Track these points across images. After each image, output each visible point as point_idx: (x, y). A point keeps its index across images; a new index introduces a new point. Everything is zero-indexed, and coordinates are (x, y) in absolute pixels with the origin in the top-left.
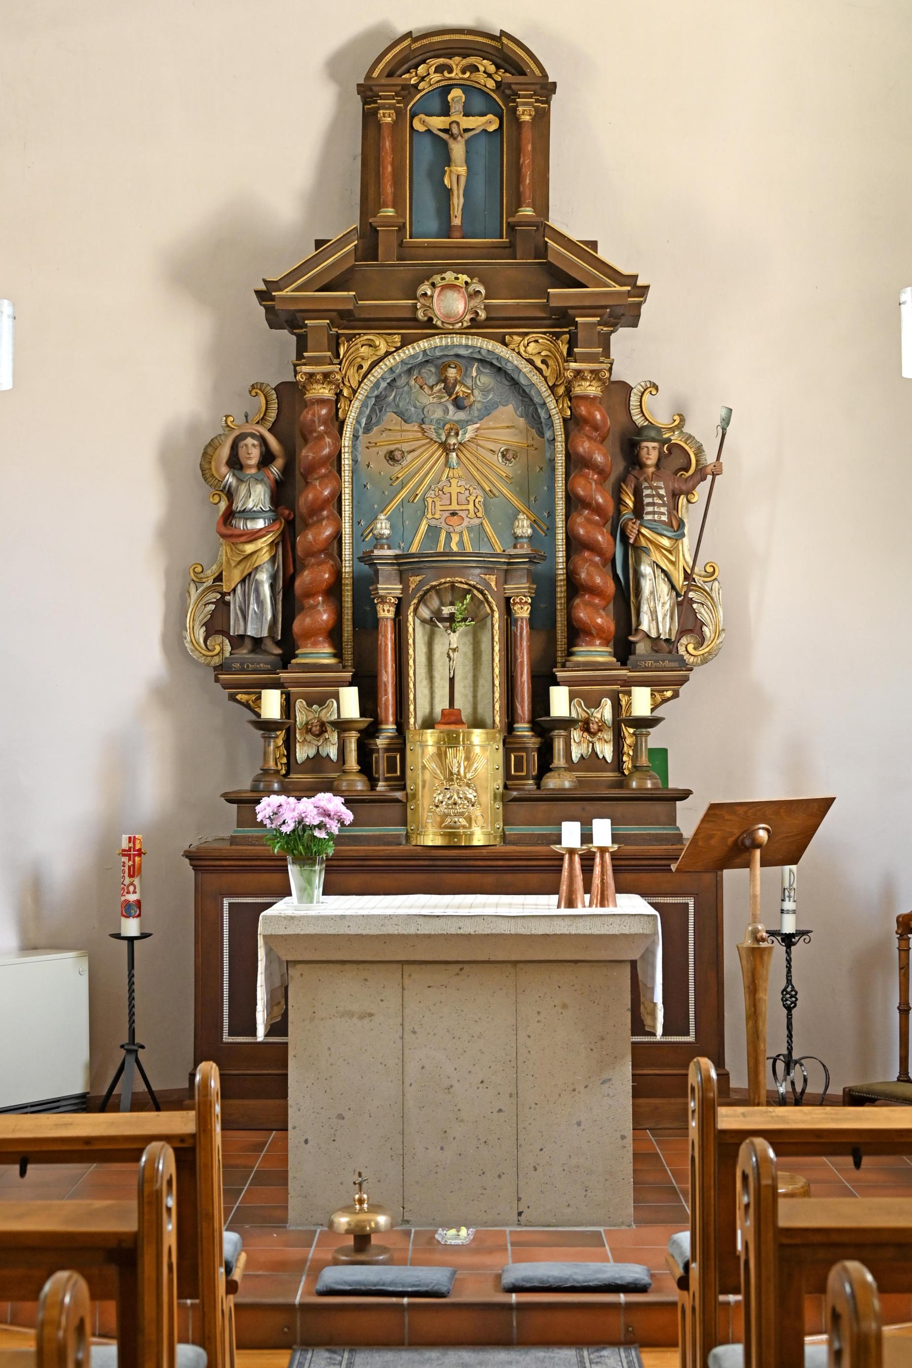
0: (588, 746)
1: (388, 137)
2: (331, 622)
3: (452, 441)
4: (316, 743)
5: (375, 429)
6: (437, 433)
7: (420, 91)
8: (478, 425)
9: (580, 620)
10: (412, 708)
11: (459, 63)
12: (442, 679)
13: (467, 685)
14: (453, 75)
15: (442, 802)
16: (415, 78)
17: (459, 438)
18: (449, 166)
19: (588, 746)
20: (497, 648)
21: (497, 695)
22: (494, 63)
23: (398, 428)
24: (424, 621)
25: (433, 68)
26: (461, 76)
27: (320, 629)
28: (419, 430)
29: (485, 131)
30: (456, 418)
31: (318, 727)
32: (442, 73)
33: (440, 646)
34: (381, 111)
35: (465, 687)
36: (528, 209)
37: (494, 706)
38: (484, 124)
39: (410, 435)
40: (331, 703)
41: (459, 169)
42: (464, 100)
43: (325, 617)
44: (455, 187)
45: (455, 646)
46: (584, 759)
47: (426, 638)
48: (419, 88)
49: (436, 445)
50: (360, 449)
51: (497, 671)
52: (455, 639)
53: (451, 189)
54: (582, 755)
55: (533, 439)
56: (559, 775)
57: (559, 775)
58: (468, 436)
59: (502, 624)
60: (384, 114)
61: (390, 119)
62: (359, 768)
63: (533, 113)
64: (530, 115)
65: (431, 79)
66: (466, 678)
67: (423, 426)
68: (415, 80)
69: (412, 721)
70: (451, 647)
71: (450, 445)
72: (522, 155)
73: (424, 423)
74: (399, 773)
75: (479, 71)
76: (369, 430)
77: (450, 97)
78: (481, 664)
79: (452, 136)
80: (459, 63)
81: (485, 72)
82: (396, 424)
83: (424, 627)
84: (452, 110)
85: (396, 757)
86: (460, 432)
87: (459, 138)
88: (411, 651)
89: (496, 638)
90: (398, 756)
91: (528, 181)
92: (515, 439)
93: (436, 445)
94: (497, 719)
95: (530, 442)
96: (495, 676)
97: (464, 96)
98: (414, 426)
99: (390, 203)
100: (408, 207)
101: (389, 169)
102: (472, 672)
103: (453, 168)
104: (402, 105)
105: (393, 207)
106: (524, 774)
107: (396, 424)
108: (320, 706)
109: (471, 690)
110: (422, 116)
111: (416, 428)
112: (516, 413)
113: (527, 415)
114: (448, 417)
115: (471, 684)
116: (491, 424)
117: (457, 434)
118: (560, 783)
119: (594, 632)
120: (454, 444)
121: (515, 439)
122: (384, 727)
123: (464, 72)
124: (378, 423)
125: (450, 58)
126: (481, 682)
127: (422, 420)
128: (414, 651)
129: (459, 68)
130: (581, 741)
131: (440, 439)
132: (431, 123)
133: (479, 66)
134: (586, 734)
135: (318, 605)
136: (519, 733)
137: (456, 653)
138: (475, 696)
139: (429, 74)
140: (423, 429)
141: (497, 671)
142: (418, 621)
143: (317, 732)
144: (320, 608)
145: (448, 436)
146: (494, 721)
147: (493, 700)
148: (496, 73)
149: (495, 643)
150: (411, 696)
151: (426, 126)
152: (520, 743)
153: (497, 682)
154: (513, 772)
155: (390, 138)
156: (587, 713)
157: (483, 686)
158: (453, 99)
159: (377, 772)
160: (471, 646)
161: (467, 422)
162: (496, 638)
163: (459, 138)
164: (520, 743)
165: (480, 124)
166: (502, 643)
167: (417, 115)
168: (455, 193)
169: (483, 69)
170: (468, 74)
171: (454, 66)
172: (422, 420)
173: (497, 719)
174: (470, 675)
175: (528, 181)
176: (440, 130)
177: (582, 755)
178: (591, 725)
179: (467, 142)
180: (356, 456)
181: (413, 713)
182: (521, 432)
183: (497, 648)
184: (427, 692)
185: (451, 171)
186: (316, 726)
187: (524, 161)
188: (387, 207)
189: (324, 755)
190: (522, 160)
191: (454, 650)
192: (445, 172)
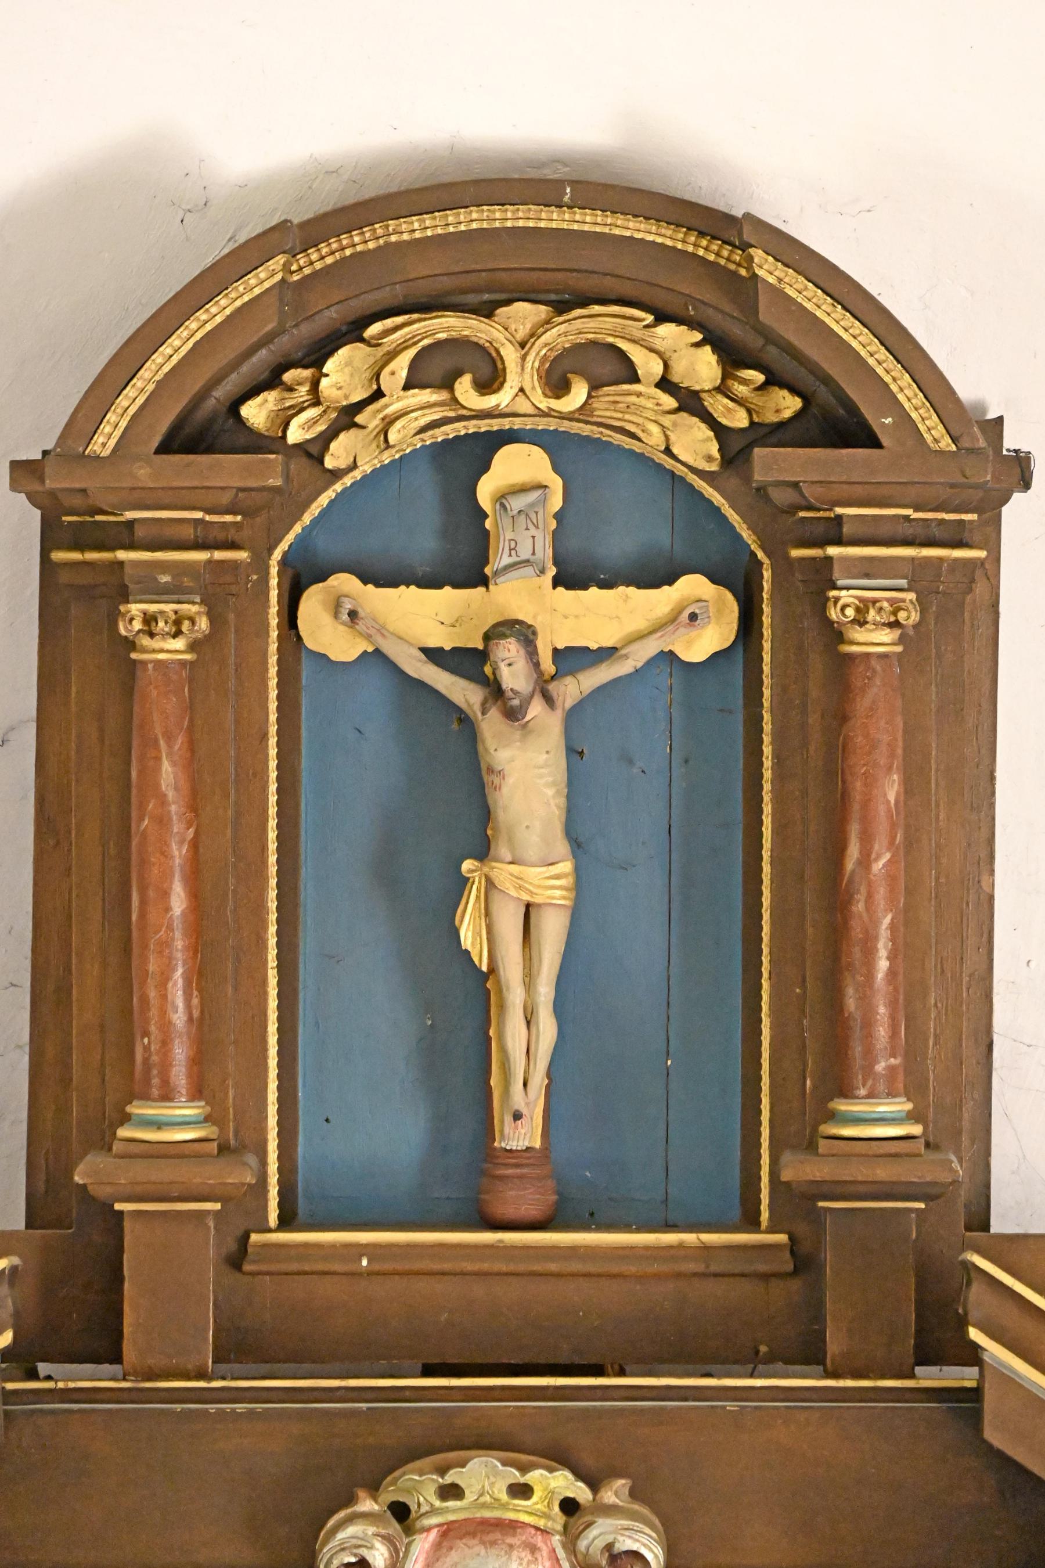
1: (169, 738)
7: (336, 475)
11: (533, 335)
14: (502, 399)
16: (312, 413)
18: (483, 852)
22: (713, 340)
25: (401, 365)
26: (544, 404)
29: (669, 657)
32: (448, 384)
34: (135, 608)
36: (884, 1108)
38: (657, 628)
41: (535, 874)
42: (556, 502)
44: (512, 970)
48: (329, 463)
53: (492, 970)
60: (149, 619)
61: (179, 644)
63: (910, 617)
64: (895, 624)
65: (389, 422)
68: (315, 421)
72: (854, 830)
75: (635, 379)
77: (486, 489)
79: (495, 691)
80: (533, 335)
81: (665, 384)
84: (500, 559)
87: (536, 709)
91: (883, 965)
97: (556, 483)
99: (180, 1076)
100: (273, 1062)
101: (178, 902)
103: (502, 873)
104: (243, 555)
105: (197, 1093)
110: (345, 582)
123: (559, 387)
125: (487, 311)
129: (533, 360)
132: (395, 624)
133: (637, 355)
139: (378, 394)
148: (721, 389)
151: (368, 637)
155: (180, 741)
158: (501, 499)
163: (536, 709)
165: (639, 623)
167: (323, 578)
168: (516, 997)
169: (658, 369)
170: (579, 393)
171: (510, 355)
175: (883, 965)
176: (433, 655)
179: (572, 717)
185: (490, 884)
187: (865, 861)
188: (167, 1096)
190: (853, 851)
192: (463, 883)
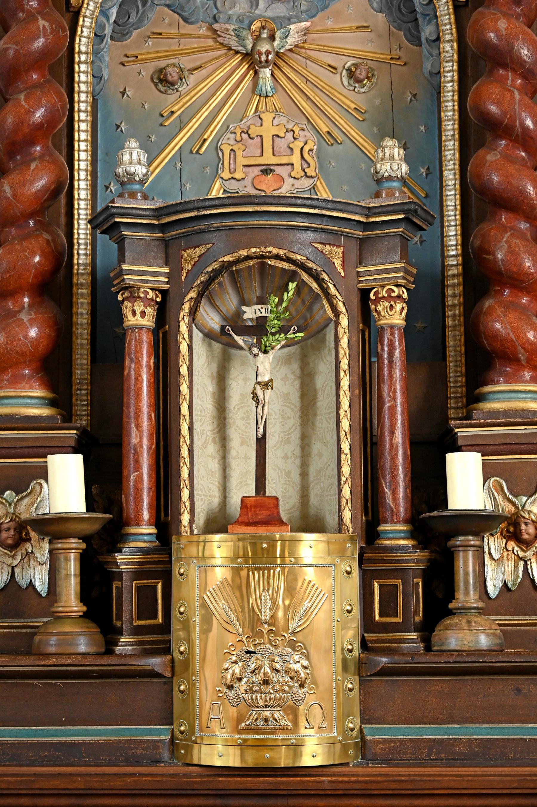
0: (516, 566)
2: (43, 342)
3: (264, 47)
4: (9, 561)
5: (135, 33)
6: (238, 36)
8: (308, 24)
9: (495, 336)
10: (185, 494)
12: (243, 443)
13: (290, 454)
15: (240, 679)
17: (276, 43)
19: (516, 566)
20: (345, 382)
21: (346, 470)
23: (175, 31)
24: (209, 335)
27: (23, 354)
28: (209, 33)
30: (270, 14)
31: (12, 532)
33: (241, 382)
35: (286, 457)
37: (340, 491)
39: (195, 44)
40: (38, 488)
43: (33, 332)
45: (266, 378)
46: (509, 590)
47: (214, 366)
49: (239, 58)
50: (107, 59)
51: (345, 424)
52: (267, 366)
54: (505, 584)
55: (400, 48)
56: (469, 622)
57: (469, 622)
58: (290, 41)
59: (354, 339)
62: (85, 609)
66: (288, 441)
67: (216, 26)
69: (185, 518)
70: (260, 379)
71: (260, 54)
73: (217, 22)
74: (160, 620)
76: (127, 33)
78: (315, 415)
82: (170, 25)
83: (210, 345)
85: (155, 588)
86: (278, 34)
88: (184, 389)
89: (344, 364)
90: (159, 586)
92: (370, 47)
93: (239, 58)
94: (347, 515)
95: (396, 53)
96: (342, 434)
98: (201, 27)
102: (298, 428)
106: (398, 620)
107: (170, 25)
108: (17, 494)
109: (298, 462)
111: (203, 31)
112: (371, 5)
113: (390, 9)
114: (257, 12)
115: (298, 452)
116: (329, 23)
117: (272, 38)
118: (471, 638)
119: (522, 356)
120: (268, 53)
121: (370, 47)
122: (133, 530)
124: (139, 23)
126: (316, 447)
127: (214, 17)
128: (190, 388)
130: (502, 557)
131: (244, 46)
134: (511, 545)
135: (20, 311)
136: (388, 542)
137: (268, 392)
138: (304, 475)
140: (215, 31)
141: (345, 424)
142: (197, 335)
143: (10, 542)
144: (24, 317)
145: (258, 39)
146: (341, 519)
147: (339, 480)
149: (342, 374)
150: (185, 473)
152: (391, 561)
153: (345, 447)
154: (377, 617)
156: (514, 505)
157: (320, 455)
159: (119, 617)
160: (297, 383)
161: (289, 19)
162: (344, 364)
164: (391, 561)
166: (355, 374)
172: (214, 17)
173: (347, 515)
174: (295, 437)
177: (505, 584)
178: (523, 527)
180: (100, 70)
181: (188, 504)
182: (380, 36)
183: (345, 382)
184: (215, 465)
186: (8, 529)
189: (24, 583)
191: (265, 385)
